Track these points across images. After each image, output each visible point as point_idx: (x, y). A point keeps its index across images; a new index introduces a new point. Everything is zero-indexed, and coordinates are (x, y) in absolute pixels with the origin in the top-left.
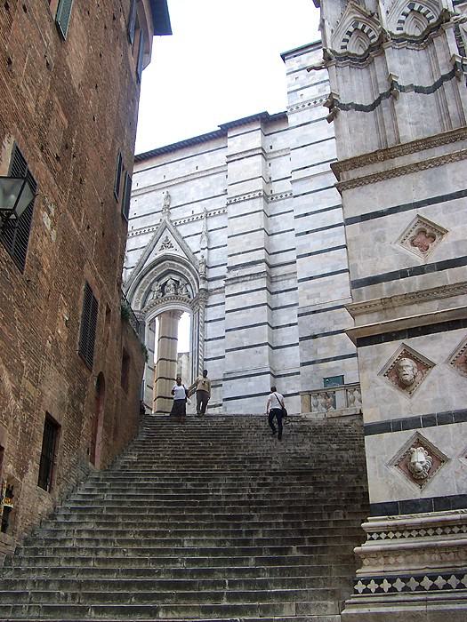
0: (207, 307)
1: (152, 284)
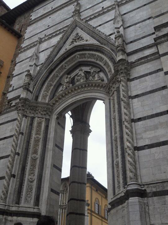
0: (130, 80)
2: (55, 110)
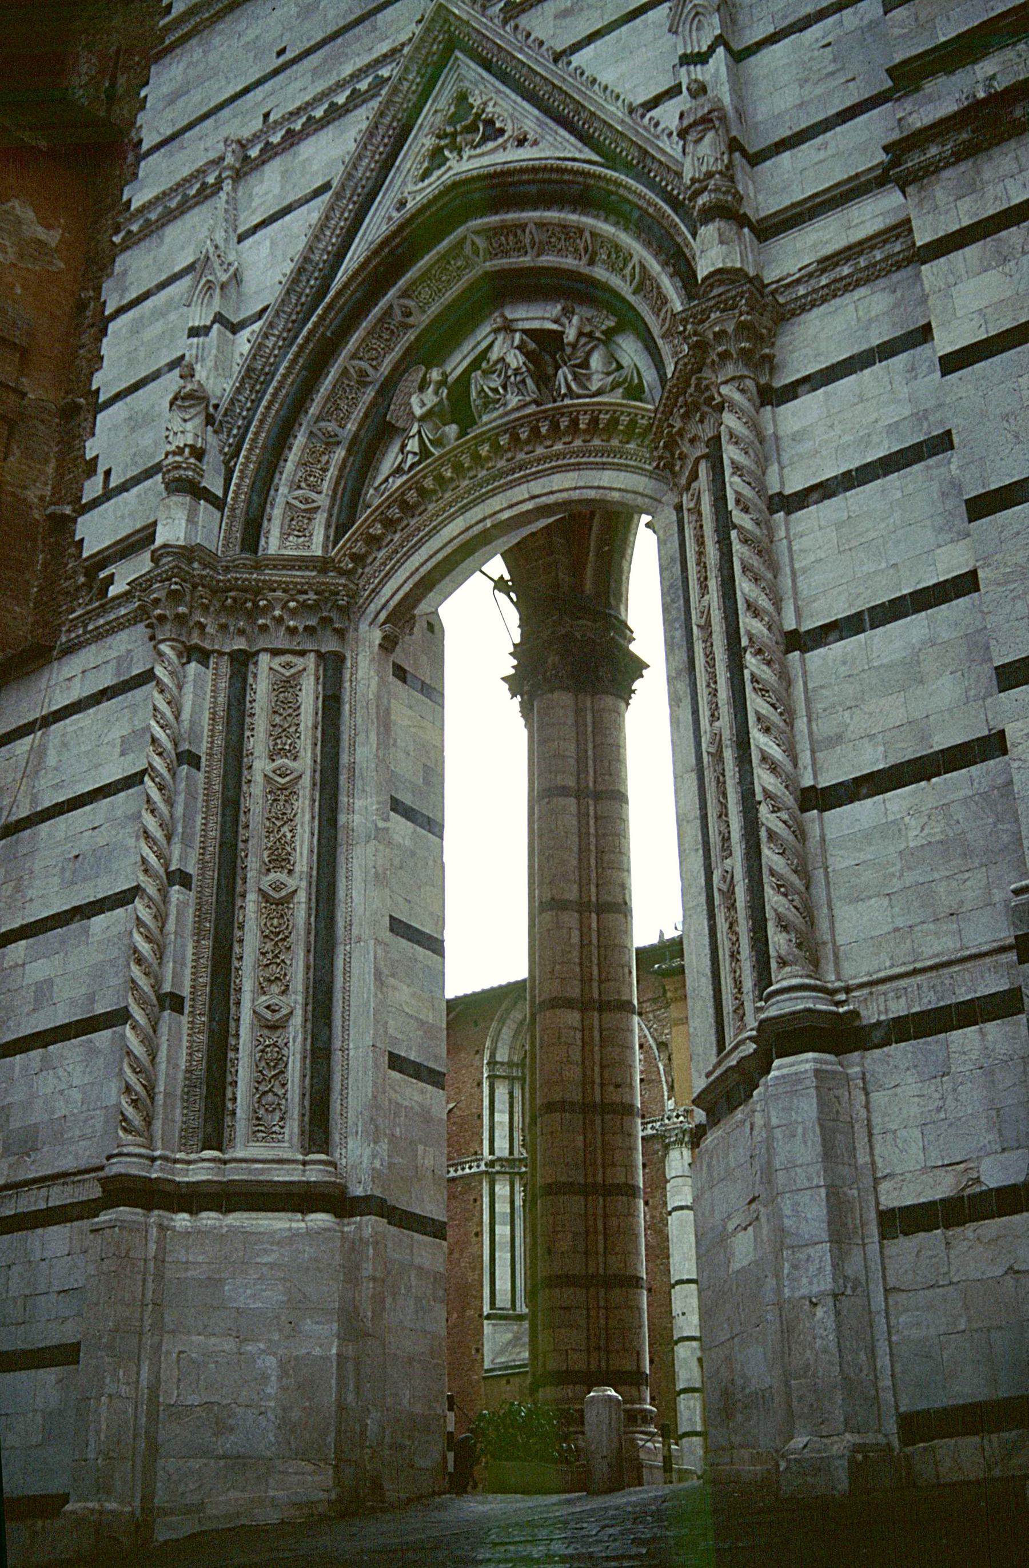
2: (370, 599)
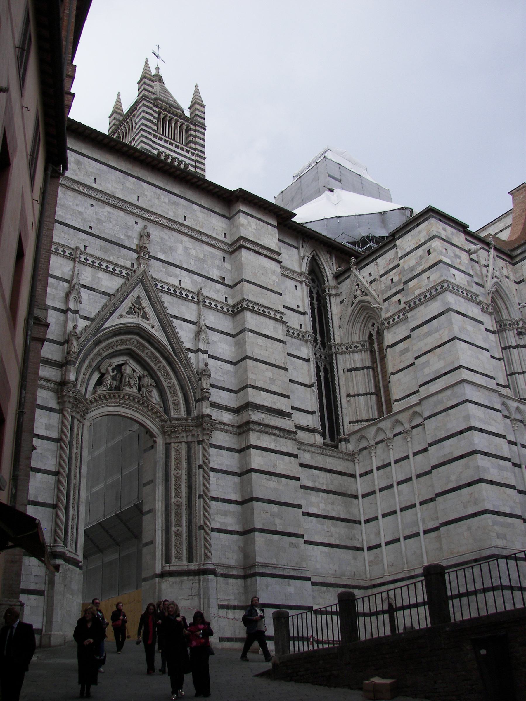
1: (103, 359)
